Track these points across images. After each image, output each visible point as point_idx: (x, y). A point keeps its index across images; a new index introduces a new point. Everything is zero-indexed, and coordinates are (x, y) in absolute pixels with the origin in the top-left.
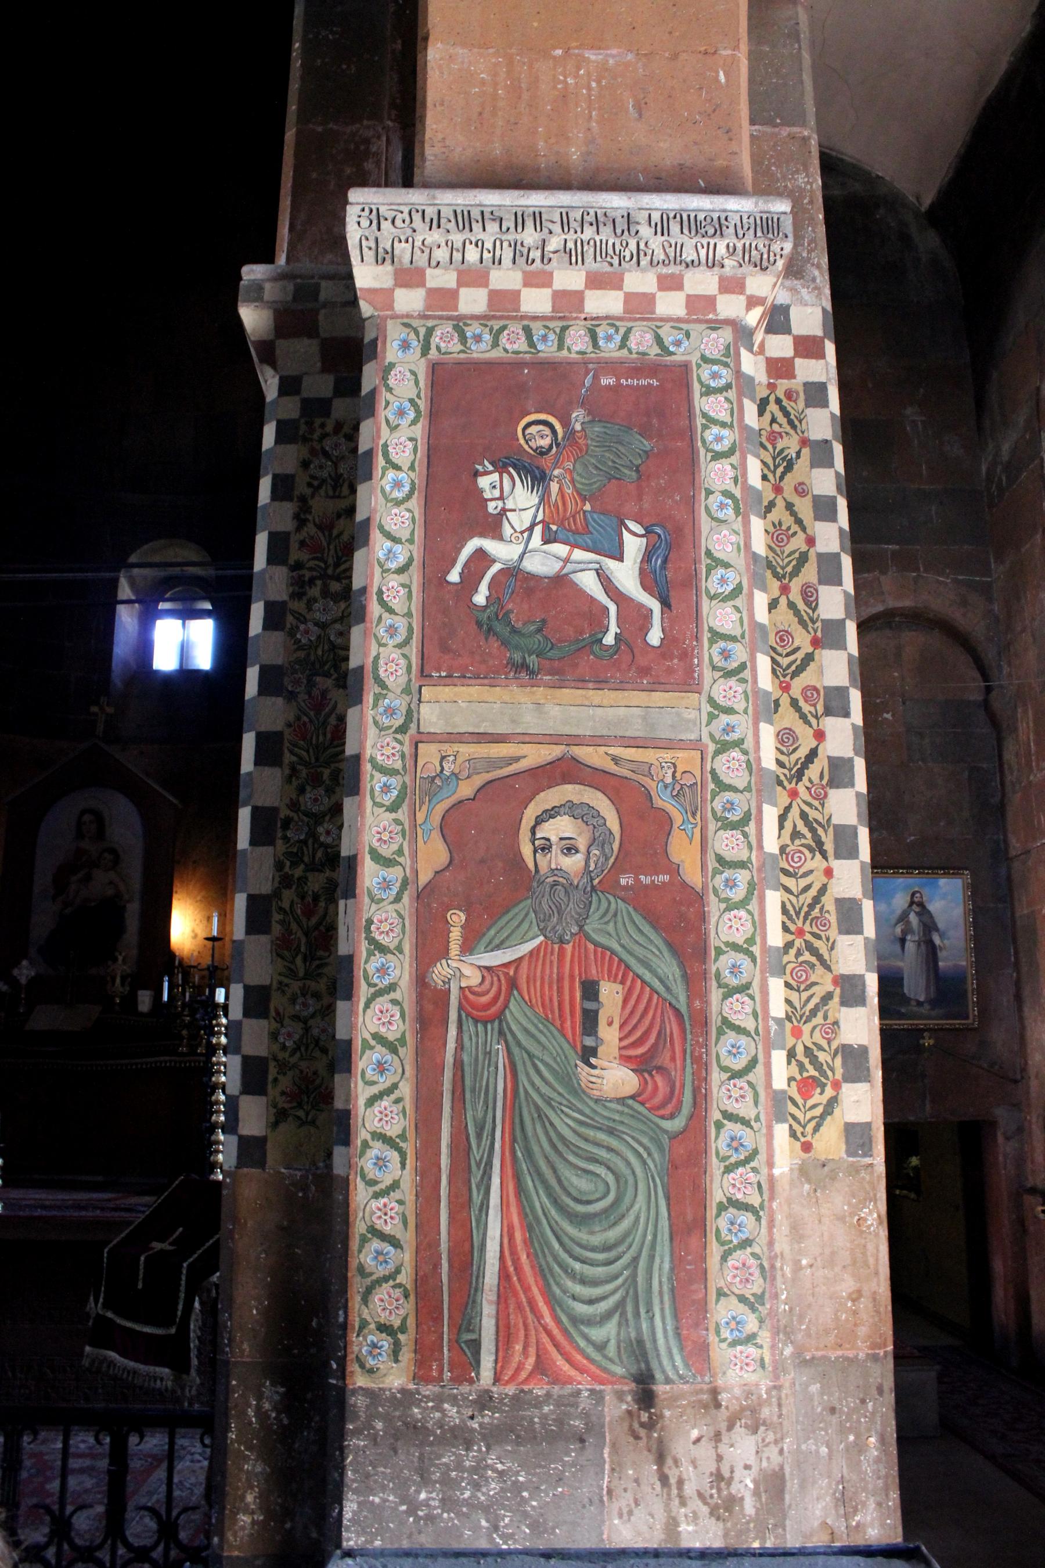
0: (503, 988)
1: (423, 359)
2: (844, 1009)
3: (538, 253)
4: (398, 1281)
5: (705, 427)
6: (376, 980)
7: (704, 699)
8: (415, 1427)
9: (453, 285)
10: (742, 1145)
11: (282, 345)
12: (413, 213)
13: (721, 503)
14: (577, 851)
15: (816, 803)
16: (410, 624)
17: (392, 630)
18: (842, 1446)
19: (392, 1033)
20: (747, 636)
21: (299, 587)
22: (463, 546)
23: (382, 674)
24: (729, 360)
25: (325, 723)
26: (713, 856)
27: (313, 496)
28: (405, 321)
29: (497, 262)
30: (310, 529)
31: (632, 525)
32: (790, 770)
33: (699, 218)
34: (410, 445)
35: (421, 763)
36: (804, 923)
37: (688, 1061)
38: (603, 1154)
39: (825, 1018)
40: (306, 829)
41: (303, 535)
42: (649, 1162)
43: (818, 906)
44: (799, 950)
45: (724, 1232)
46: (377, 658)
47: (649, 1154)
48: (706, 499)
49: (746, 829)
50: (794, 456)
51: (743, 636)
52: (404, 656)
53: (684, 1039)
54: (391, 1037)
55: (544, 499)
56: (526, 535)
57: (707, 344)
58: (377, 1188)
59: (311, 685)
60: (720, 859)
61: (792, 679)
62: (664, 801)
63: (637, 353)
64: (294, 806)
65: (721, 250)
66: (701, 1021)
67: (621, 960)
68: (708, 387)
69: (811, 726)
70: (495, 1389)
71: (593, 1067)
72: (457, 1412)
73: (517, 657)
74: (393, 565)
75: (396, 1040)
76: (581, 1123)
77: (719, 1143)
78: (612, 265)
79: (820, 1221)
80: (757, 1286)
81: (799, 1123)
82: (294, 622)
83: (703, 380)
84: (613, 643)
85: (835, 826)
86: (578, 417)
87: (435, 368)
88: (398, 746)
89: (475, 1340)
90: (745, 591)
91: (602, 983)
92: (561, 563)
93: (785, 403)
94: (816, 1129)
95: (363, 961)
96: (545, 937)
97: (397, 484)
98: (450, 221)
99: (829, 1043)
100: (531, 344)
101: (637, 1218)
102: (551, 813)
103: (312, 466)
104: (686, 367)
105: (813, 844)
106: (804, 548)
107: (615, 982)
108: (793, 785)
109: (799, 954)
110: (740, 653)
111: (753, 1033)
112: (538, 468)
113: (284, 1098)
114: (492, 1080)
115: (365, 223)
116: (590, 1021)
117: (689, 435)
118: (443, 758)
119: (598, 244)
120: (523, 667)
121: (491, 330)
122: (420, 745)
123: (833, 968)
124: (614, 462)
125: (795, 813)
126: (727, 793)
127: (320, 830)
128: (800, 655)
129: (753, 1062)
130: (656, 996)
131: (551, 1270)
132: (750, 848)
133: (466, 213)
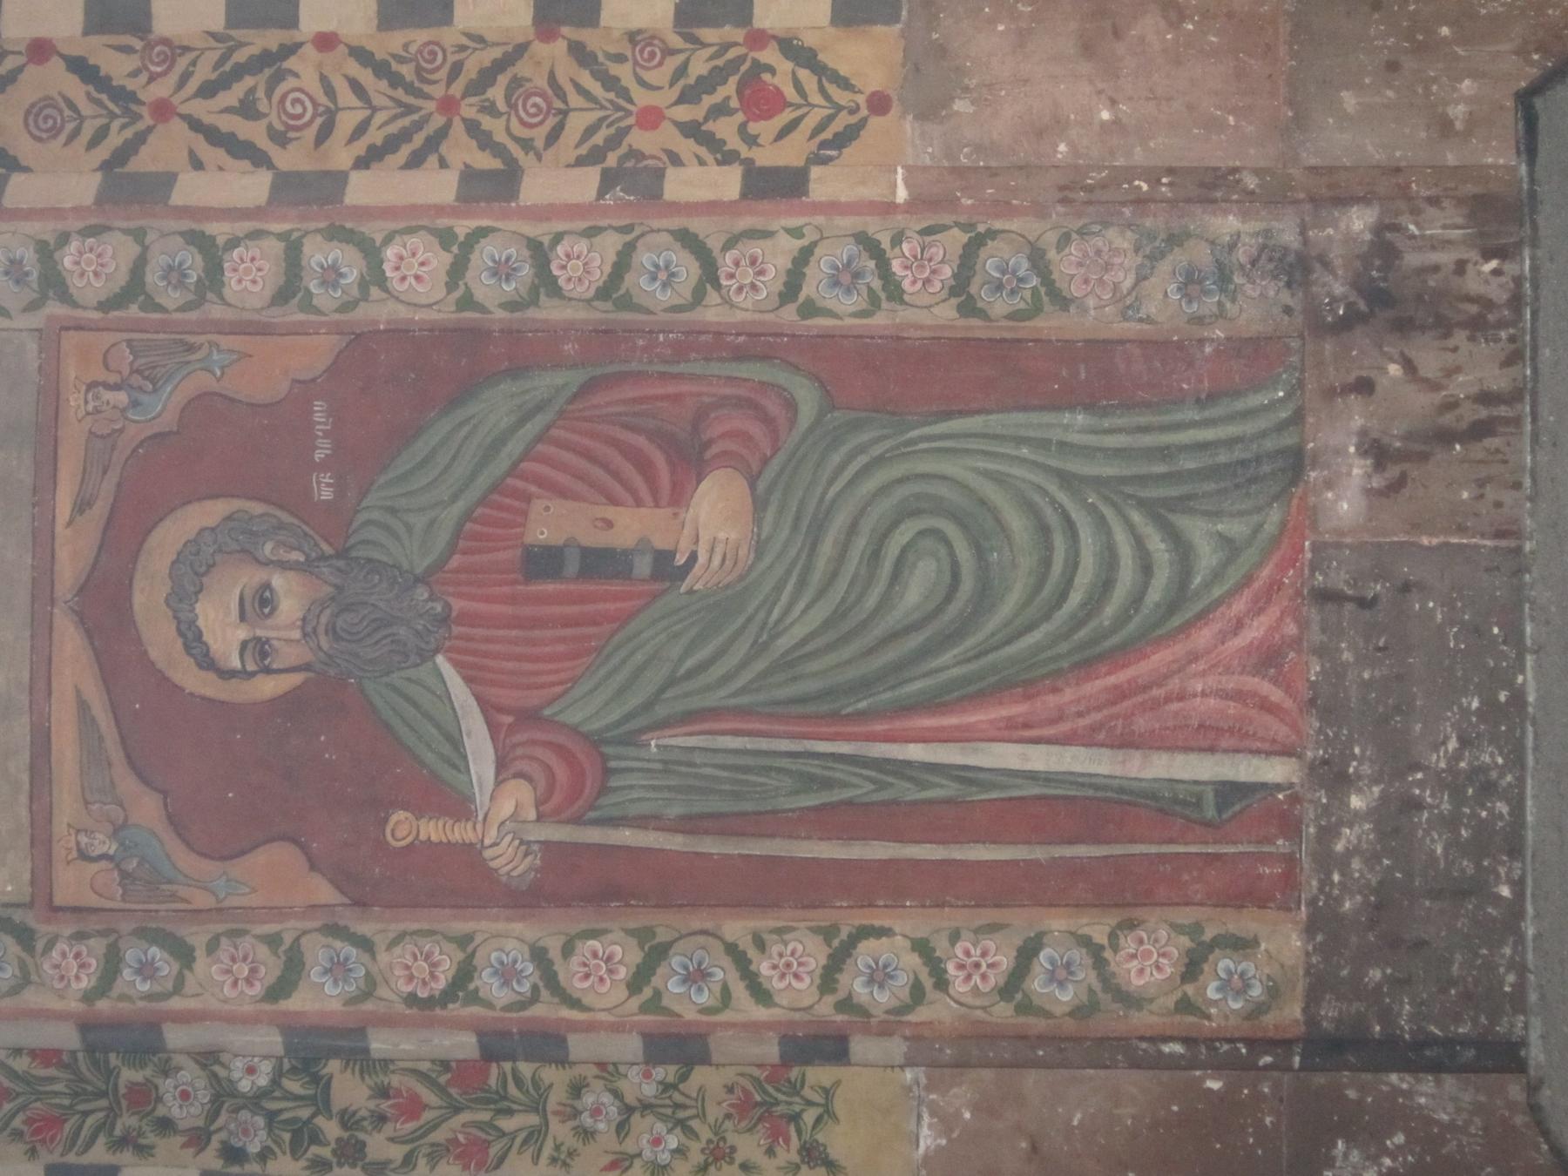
0: (539, 736)
2: (606, 17)
4: (1105, 941)
6: (526, 988)
8: (1378, 907)
10: (849, 262)
14: (267, 586)
15: (182, 63)
18: (1460, 51)
19: (625, 954)
26: (275, 311)
32: (113, 116)
35: (94, 901)
36: (428, 97)
37: (682, 368)
38: (861, 544)
39: (620, 58)
40: (244, 1115)
42: (877, 450)
43: (395, 66)
44: (482, 110)
45: (1017, 303)
47: (861, 449)
49: (220, 241)
53: (638, 377)
54: (636, 957)
58: (928, 982)
60: (283, 296)
64: (198, 1139)
66: (604, 338)
67: (483, 501)
69: (20, 69)
70: (1309, 754)
71: (693, 557)
72: (1351, 827)
75: (642, 949)
76: (802, 583)
79: (1026, 81)
80: (1122, 240)
81: (830, 119)
85: (231, 22)
88: (61, 946)
89: (1217, 793)
91: (528, 540)
94: (845, 84)
95: (490, 1013)
96: (436, 651)
99: (670, 52)
101: (987, 474)
102: (193, 640)
105: (268, 72)
107: (525, 514)
108: (144, 111)
109: (490, 109)
111: (628, 238)
113: (779, 1150)
114: (719, 759)
118: (84, 856)
123: (521, 40)
125: (202, 109)
126: (149, 278)
127: (245, 1085)
129: (687, 239)
130: (554, 432)
131: (1083, 646)
132: (256, 235)
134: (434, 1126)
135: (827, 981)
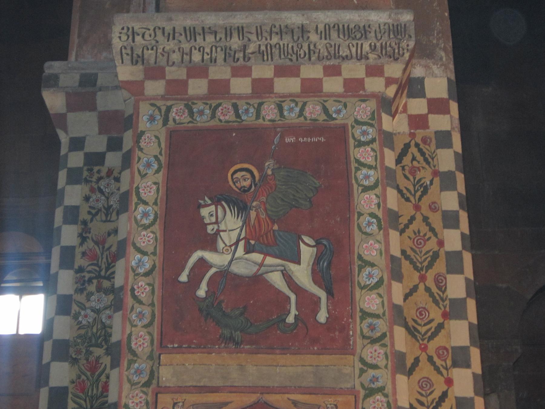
1: (164, 128)
3: (241, 55)
5: (357, 169)
7: (356, 359)
9: (185, 77)
11: (71, 116)
12: (157, 30)
13: (369, 222)
16: (153, 312)
17: (141, 315)
20: (387, 314)
22: (190, 257)
23: (133, 346)
24: (374, 122)
25: (98, 380)
27: (92, 220)
28: (152, 102)
29: (214, 61)
30: (90, 244)
31: (306, 239)
33: (350, 27)
34: (155, 187)
41: (84, 247)
46: (130, 335)
48: (358, 219)
50: (428, 183)
51: (384, 314)
52: (149, 333)
55: (246, 222)
56: (233, 248)
57: (358, 112)
59: (89, 353)
61: (428, 341)
63: (310, 120)
65: (366, 47)
68: (359, 141)
69: (442, 375)
73: (227, 332)
74: (141, 271)
78: (291, 60)
82: (77, 309)
83: (356, 136)
84: (293, 321)
86: (270, 164)
87: (172, 135)
88: (144, 397)
90: (386, 282)
92: (257, 267)
93: (422, 146)
97: (145, 215)
98: (181, 35)
100: (238, 116)
103: (91, 200)
104: (344, 128)
106: (436, 248)
110: (382, 325)
112: (241, 201)
115: (124, 38)
117: (346, 175)
119: (282, 47)
120: (231, 339)
121: (210, 107)
122: (159, 395)
124: (294, 196)
128: (434, 325)
133: (192, 29)
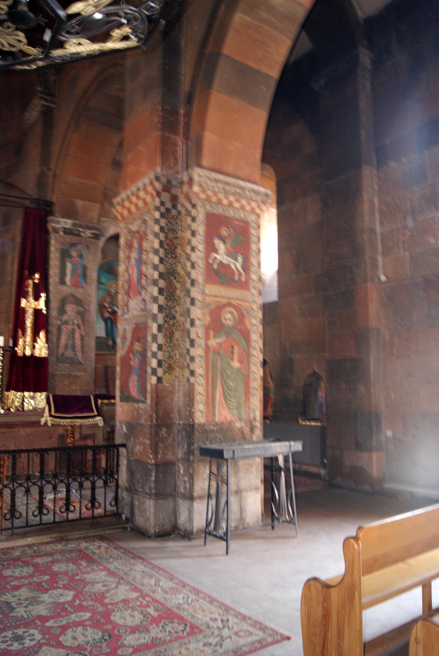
21: (166, 254)
25: (172, 287)
38: (235, 379)
55: (226, 248)
62: (245, 313)
77: (251, 377)
116: (232, 353)
127: (172, 311)
134: (168, 331)
135: (200, 375)
